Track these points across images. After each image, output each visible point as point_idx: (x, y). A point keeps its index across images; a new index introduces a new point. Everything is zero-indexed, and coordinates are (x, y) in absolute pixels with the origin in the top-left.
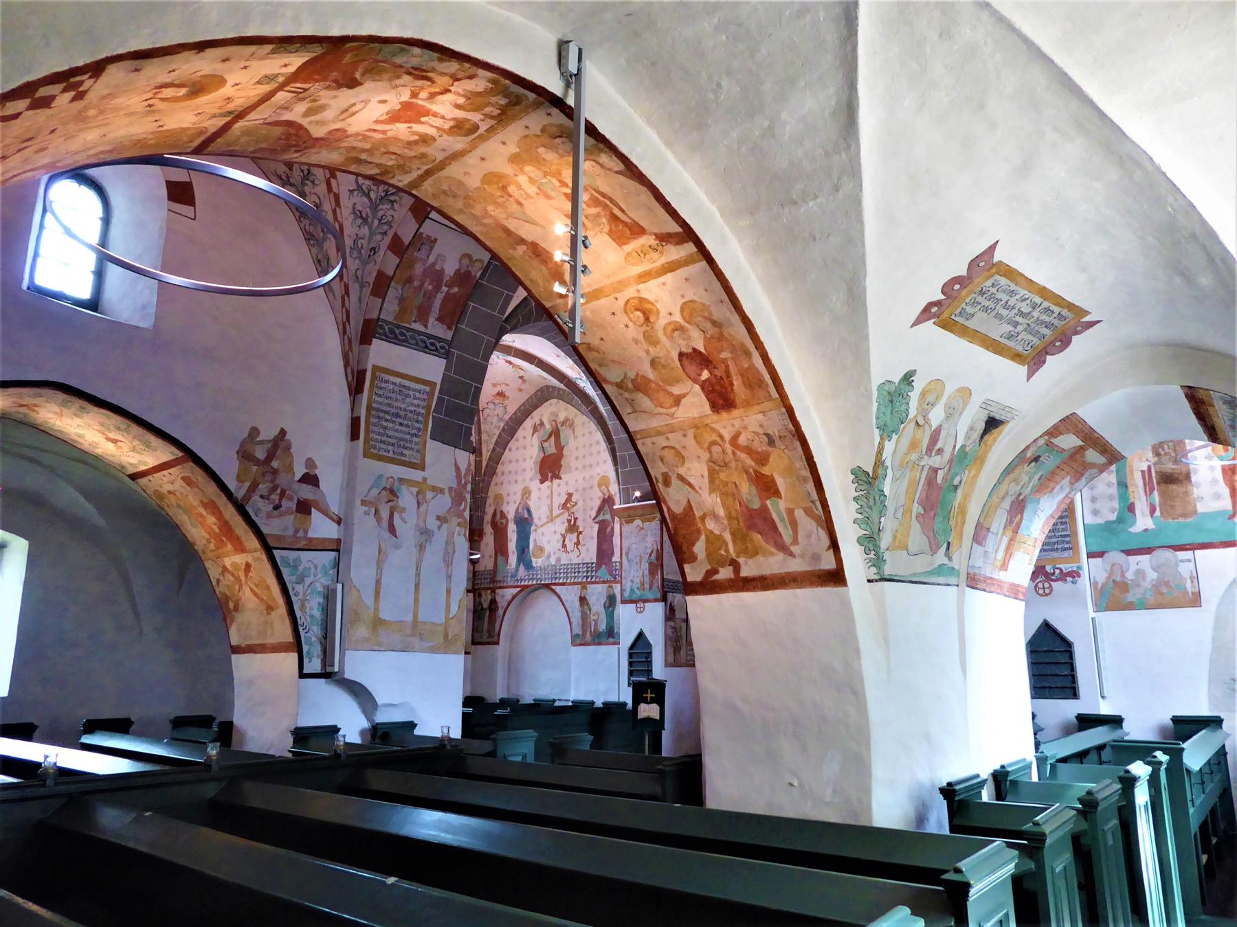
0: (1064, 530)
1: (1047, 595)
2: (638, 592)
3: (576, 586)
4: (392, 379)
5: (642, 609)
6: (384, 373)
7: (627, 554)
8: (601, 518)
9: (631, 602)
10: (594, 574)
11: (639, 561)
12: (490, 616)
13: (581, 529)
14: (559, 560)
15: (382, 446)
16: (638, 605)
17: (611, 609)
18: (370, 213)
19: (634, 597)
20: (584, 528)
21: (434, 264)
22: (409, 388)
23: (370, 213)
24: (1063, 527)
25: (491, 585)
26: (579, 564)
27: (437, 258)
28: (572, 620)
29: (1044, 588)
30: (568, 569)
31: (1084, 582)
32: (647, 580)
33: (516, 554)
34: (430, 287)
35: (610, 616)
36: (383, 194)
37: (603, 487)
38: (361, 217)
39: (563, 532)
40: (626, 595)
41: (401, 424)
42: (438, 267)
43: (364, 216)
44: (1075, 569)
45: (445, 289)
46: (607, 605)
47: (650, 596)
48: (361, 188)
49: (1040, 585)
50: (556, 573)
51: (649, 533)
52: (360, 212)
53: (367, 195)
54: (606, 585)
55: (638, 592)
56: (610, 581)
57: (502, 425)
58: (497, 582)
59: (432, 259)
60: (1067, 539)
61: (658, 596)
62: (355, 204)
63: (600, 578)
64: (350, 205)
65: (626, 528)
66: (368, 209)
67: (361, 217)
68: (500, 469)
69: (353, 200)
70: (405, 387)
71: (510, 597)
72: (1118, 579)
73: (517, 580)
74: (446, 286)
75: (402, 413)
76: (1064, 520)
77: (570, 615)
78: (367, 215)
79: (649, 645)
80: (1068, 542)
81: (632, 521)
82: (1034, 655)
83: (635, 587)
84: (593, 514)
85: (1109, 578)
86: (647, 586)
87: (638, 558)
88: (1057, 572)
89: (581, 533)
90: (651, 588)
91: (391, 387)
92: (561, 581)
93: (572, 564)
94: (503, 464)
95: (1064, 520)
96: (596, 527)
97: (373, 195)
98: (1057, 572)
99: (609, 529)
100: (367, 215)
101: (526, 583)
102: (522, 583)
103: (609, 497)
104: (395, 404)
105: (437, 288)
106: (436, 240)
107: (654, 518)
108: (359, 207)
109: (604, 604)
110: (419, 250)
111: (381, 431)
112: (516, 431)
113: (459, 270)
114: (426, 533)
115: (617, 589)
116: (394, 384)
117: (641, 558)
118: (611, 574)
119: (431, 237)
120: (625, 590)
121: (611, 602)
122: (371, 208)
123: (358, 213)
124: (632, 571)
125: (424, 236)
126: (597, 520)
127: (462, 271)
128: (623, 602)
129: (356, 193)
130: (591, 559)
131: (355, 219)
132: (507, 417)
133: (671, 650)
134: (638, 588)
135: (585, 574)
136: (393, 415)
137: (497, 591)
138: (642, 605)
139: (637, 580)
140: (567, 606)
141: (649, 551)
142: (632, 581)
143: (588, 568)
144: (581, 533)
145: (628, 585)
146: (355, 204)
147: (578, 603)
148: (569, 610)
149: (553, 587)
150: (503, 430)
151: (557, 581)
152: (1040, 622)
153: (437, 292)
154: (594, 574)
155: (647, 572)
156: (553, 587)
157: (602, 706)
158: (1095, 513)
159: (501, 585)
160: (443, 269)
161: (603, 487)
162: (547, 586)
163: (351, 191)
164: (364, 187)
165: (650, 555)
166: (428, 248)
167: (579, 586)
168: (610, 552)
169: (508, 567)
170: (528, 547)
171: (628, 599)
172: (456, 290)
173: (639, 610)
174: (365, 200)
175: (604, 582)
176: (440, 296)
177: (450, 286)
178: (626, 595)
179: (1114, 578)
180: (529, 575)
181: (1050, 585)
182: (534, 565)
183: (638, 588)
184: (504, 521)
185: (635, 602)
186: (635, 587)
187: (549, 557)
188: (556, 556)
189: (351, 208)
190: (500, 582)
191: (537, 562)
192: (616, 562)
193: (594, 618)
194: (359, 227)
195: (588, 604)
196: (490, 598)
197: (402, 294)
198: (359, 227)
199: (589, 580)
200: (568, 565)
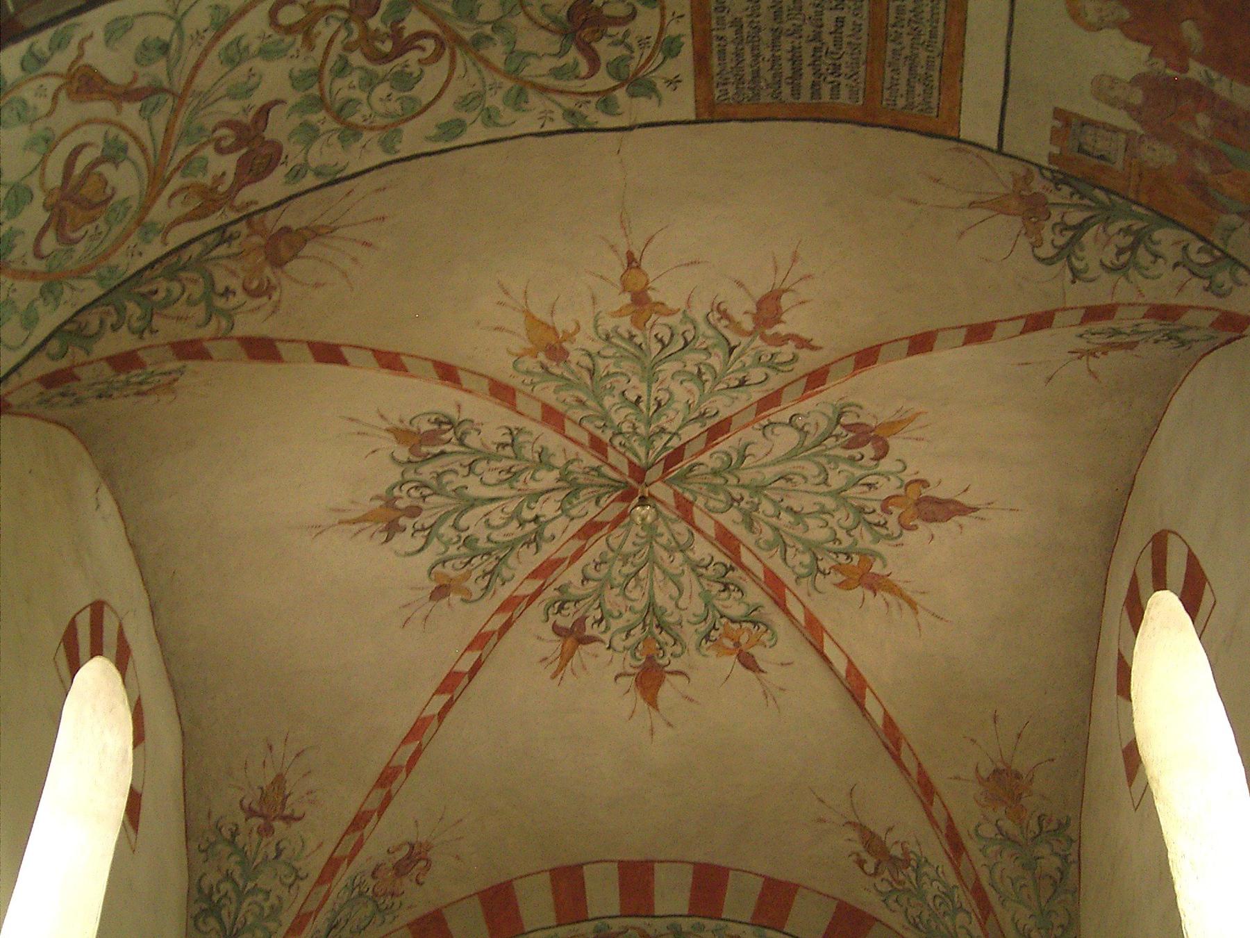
18: (1123, 224)
21: (1128, 108)
23: (1123, 224)
27: (1112, 103)
34: (1203, 120)
36: (1066, 190)
38: (1133, 248)
42: (1137, 97)
43: (1130, 239)
45: (1196, 71)
48: (1062, 248)
52: (1120, 252)
53: (1081, 228)
59: (1121, 119)
62: (1102, 264)
64: (1107, 279)
66: (1113, 229)
67: (1133, 248)
69: (1094, 270)
74: (1185, 69)
78: (1127, 231)
97: (1075, 217)
100: (1127, 231)
105: (1201, 94)
106: (1058, 113)
108: (1109, 256)
110: (1102, 157)
113: (1122, 26)
119: (1054, 131)
122: (1107, 221)
123: (1125, 257)
125: (1056, 150)
127: (1126, 14)
129: (1078, 264)
131: (1137, 267)
146: (1102, 264)
153: (1214, 96)
160: (1137, 80)
163: (1076, 275)
164: (1061, 241)
166: (1089, 130)
172: (1190, 31)
174: (1088, 237)
176: (1223, 87)
177: (1182, 53)
189: (1115, 277)
194: (1157, 256)
197: (1239, 214)
198: (1157, 256)
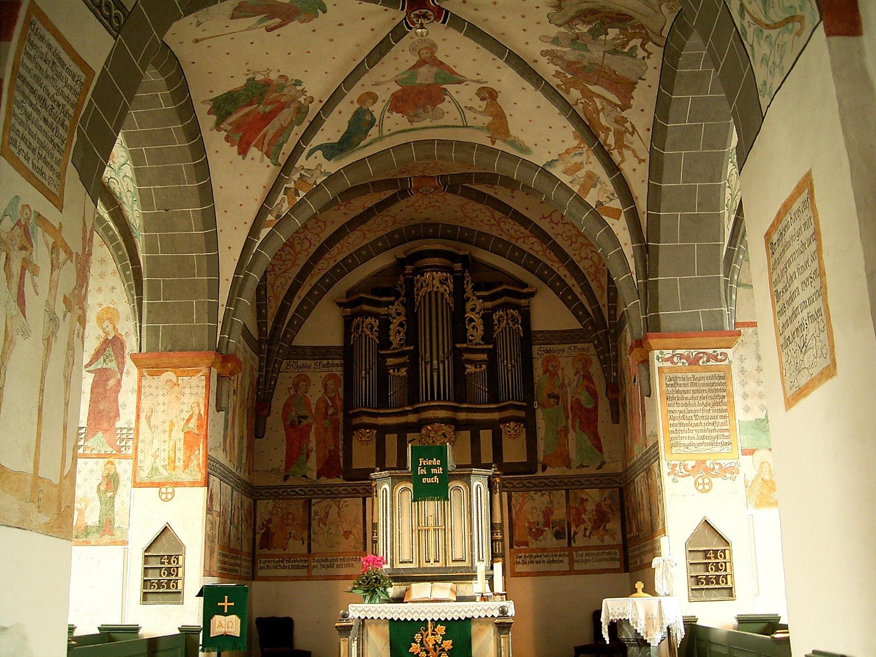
0: (723, 424)
1: (707, 491)
2: (165, 473)
4: (48, 36)
5: (170, 496)
6: (40, 20)
7: (148, 419)
8: (99, 365)
9: (152, 485)
11: (167, 429)
15: (23, 146)
16: (164, 490)
17: (109, 494)
19: (156, 479)
22: (63, 64)
24: (723, 421)
29: (704, 484)
31: (740, 478)
32: (180, 455)
35: (108, 504)
40: (143, 475)
41: (45, 121)
44: (733, 465)
46: (102, 488)
47: (186, 477)
49: (700, 481)
51: (187, 391)
54: (102, 462)
55: (161, 470)
60: (726, 434)
61: (199, 477)
65: (148, 381)
70: (60, 59)
72: (767, 477)
75: (49, 102)
76: (724, 414)
79: (180, 546)
80: (728, 437)
81: (159, 374)
82: (692, 554)
83: (159, 464)
85: (758, 475)
86: (180, 464)
87: (167, 424)
88: (717, 467)
90: (186, 466)
91: (45, 50)
95: (724, 414)
98: (717, 467)
99: (112, 383)
104: (44, 81)
107: (200, 371)
111: (23, 118)
114: (53, 319)
115: (124, 468)
116: (50, 47)
117: (172, 424)
121: (111, 482)
124: (155, 441)
126: (92, 368)
128: (136, 485)
133: (208, 553)
134: (163, 466)
136: (40, 98)
138: (170, 490)
139: (164, 455)
141: (187, 417)
142: (156, 457)
145: (146, 462)
152: (698, 520)
155: (180, 445)
157: (98, 632)
158: (747, 409)
161: (107, 323)
165: (188, 421)
168: (112, 414)
171: (147, 480)
173: (164, 497)
175: (99, 456)
178: (143, 475)
179: (763, 476)
181: (710, 480)
183: (163, 466)
185: (159, 485)
186: (159, 464)
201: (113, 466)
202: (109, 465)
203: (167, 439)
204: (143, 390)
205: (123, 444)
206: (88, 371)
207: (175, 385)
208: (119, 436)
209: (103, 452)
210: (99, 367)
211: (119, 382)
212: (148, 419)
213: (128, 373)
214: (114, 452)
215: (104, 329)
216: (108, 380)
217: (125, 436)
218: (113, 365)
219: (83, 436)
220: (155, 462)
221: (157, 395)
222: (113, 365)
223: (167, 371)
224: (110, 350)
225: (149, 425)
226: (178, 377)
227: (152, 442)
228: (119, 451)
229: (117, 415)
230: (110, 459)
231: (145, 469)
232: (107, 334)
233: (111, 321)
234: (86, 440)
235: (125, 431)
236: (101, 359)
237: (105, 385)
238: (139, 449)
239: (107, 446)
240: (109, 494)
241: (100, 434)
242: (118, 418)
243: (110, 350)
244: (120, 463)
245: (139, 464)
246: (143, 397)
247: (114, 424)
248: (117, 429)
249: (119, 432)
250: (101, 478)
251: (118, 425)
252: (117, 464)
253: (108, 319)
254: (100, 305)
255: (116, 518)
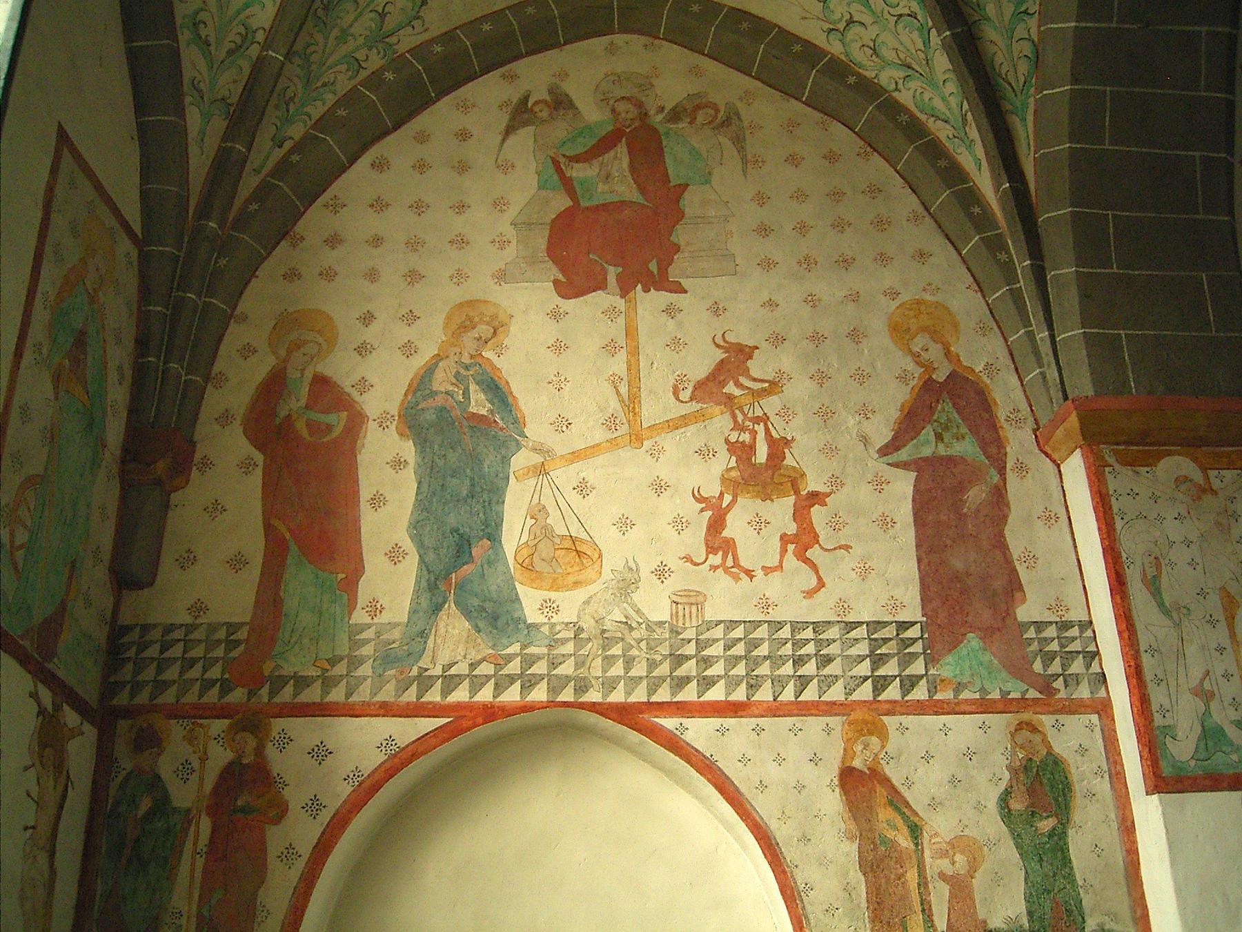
3: (815, 724)
10: (918, 667)
11: (1219, 615)
12: (218, 850)
13: (813, 483)
14: (691, 600)
17: (1046, 825)
20: (836, 482)
25: (238, 695)
26: (817, 627)
28: (800, 877)
30: (756, 644)
33: (411, 563)
37: (918, 343)
39: (712, 489)
46: (1017, 805)
50: (679, 660)
56: (1024, 703)
57: (375, 61)
58: (278, 683)
63: (959, 688)
68: (315, 221)
71: (373, 760)
73: (425, 682)
77: (790, 853)
81: (1149, 460)
84: (882, 433)
87: (1214, 600)
89: (816, 498)
92: (716, 694)
93: (780, 625)
94: (336, 207)
96: (903, 485)
99: (976, 495)
101: (485, 695)
102: (461, 695)
103: (952, 375)
109: (1004, 800)
112: (427, 103)
118: (1020, 670)
120: (1169, 730)
124: (1191, 650)
126: (903, 455)
130: (897, 606)
132: (407, 41)
135: (864, 668)
137: (278, 724)
140: (764, 806)
143: (875, 643)
144: (816, 498)
147: (831, 802)
148: (781, 831)
149: (669, 723)
150: (375, 80)
151: (689, 694)
154: (918, 667)
156: (669, 723)
159: (312, 695)
162: (624, 714)
167: (835, 722)
168: (998, 584)
169: (360, 616)
170: (492, 532)
180: (501, 662)
182: (532, 615)
184: (338, 421)
187: (627, 585)
188: (674, 583)
190: (302, 682)
191: (549, 606)
192: (1040, 626)
193: (944, 864)
195: (897, 801)
196: (220, 756)
199: (893, 692)
200: (756, 624)
201: (1037, 738)
202: (1026, 734)
203: (1227, 643)
204: (1115, 506)
205: (1056, 667)
206: (896, 465)
207: (1204, 491)
208: (1035, 646)
209: (996, 695)
210: (927, 452)
211: (999, 496)
212: (1153, 585)
213: (1022, 468)
214: (1033, 694)
215: (916, 356)
216: (961, 488)
217: (1054, 646)
218: (967, 448)
219: (918, 647)
220: (1207, 712)
221: (1160, 518)
222: (967, 448)
223: (1169, 454)
224: (946, 410)
225: (1161, 605)
226: (1204, 470)
227: (1181, 655)
228: (1046, 687)
229: (1014, 587)
230: (1026, 716)
231: (1180, 735)
232: (928, 367)
233: (935, 335)
234: (931, 660)
235: (1051, 632)
236: (928, 433)
237: (957, 506)
238: (1148, 676)
239: (1004, 674)
240: (1046, 825)
241: (973, 641)
242: (1018, 595)
243: (946, 410)
244: (1058, 726)
245: (1158, 720)
246: (1119, 524)
247: (1009, 613)
248: (1024, 626)
249: (1031, 633)
250: (1007, 775)
251: (1024, 613)
252: (1051, 734)
253: (924, 329)
254: (894, 294)
255: (1087, 901)
